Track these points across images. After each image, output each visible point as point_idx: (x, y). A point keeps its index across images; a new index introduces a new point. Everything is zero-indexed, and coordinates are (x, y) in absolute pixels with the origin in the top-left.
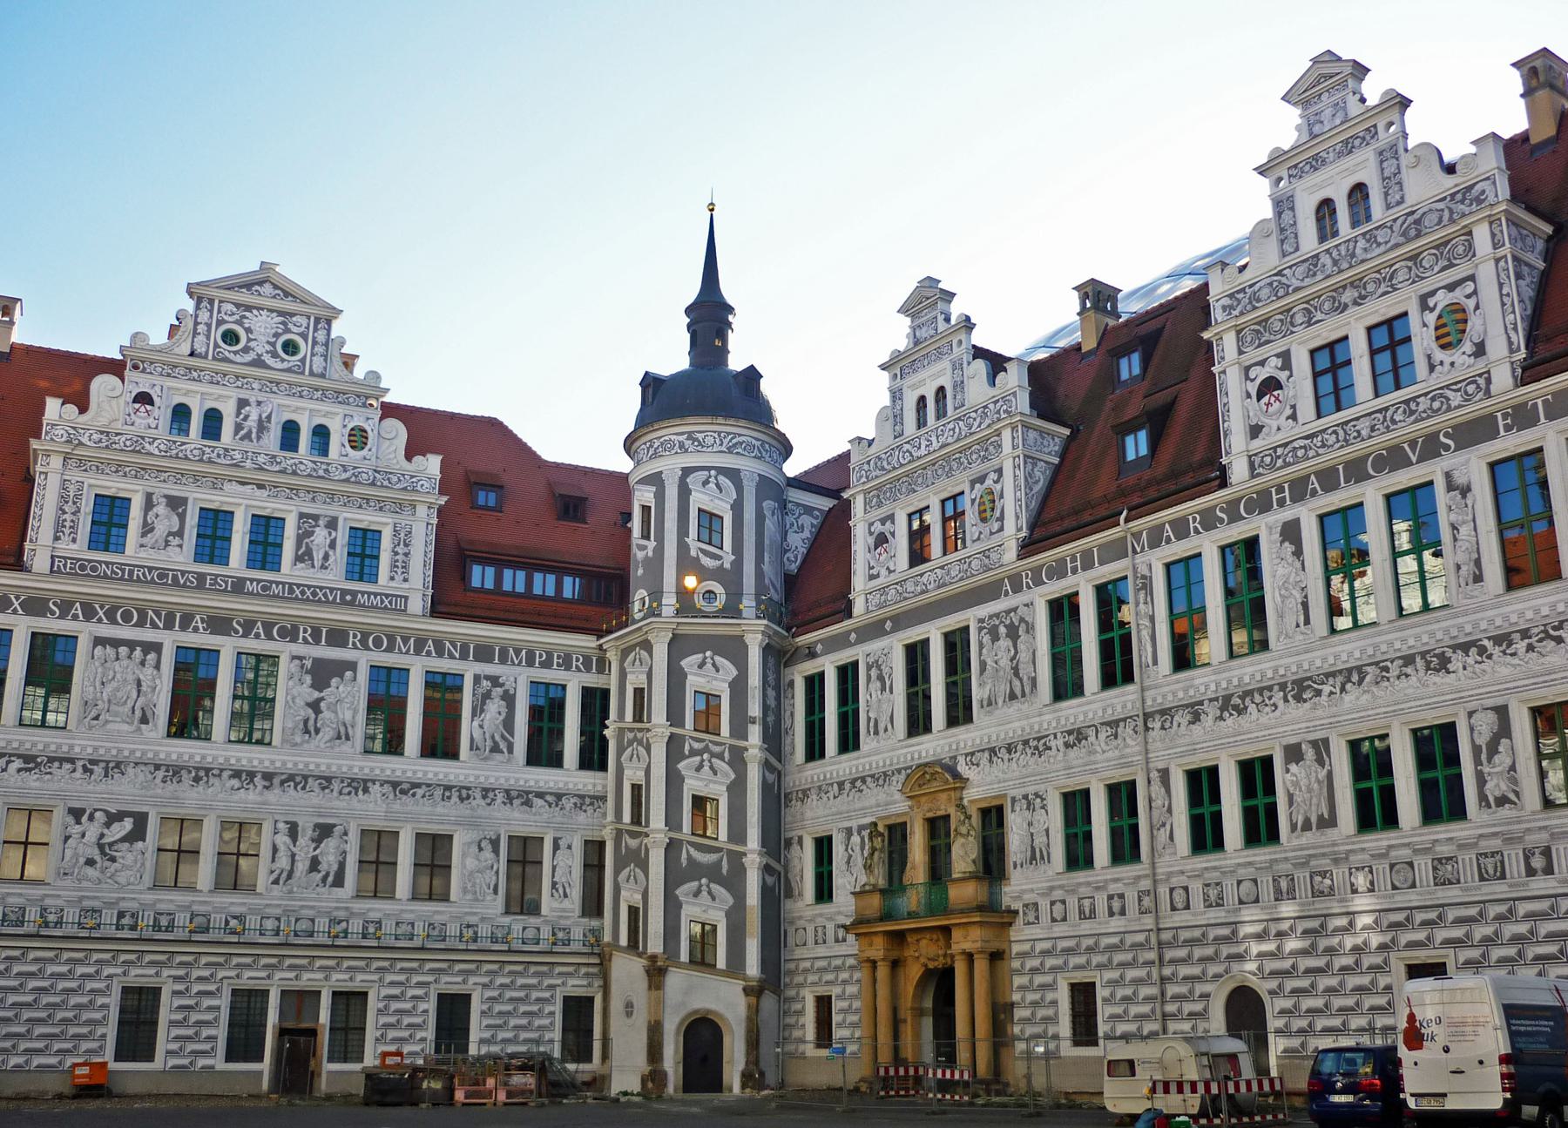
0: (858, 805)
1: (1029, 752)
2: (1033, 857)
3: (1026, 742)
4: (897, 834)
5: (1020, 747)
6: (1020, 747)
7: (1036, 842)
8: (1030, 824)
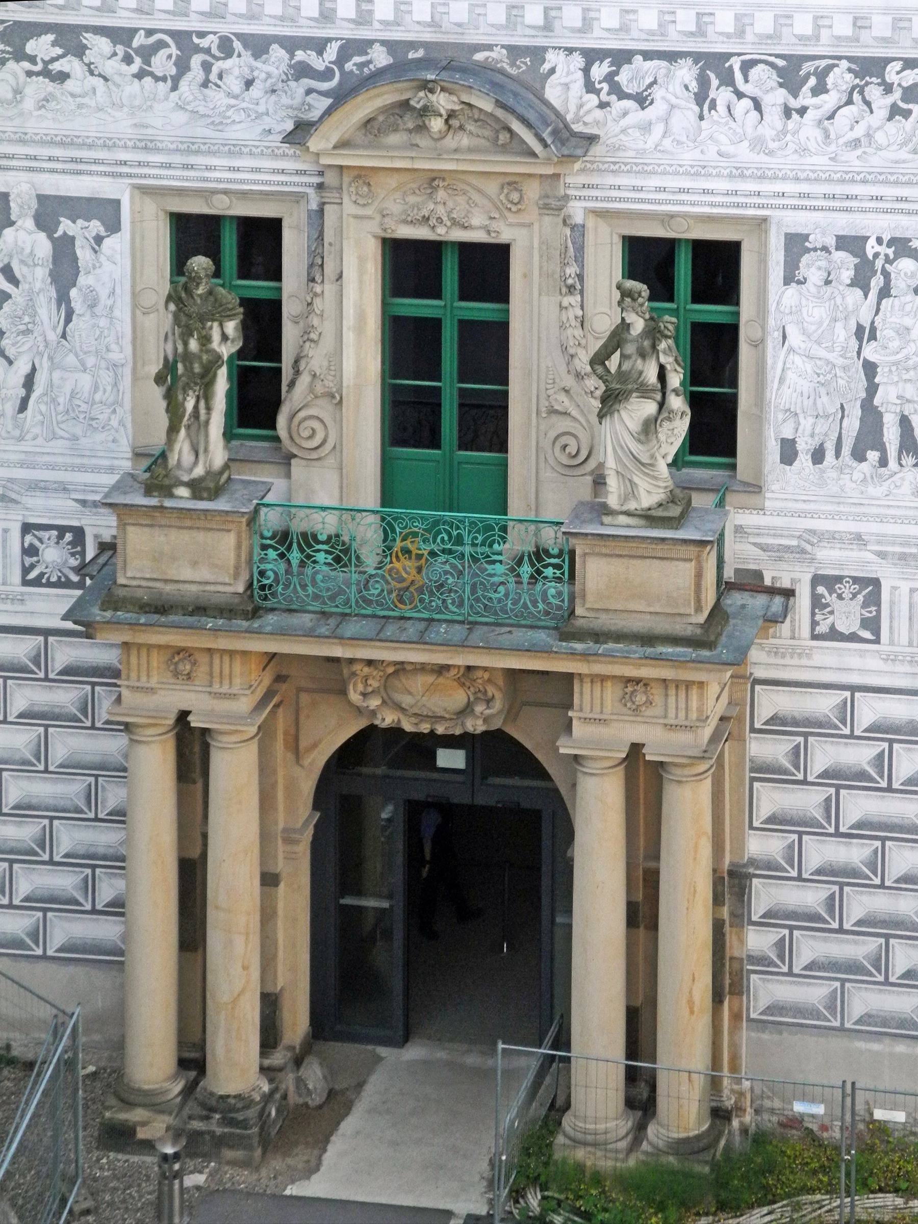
0: (42, 124)
1: (881, 102)
2: (869, 438)
3: (869, 68)
4: (231, 252)
5: (841, 78)
6: (841, 78)
7: (886, 397)
8: (865, 334)
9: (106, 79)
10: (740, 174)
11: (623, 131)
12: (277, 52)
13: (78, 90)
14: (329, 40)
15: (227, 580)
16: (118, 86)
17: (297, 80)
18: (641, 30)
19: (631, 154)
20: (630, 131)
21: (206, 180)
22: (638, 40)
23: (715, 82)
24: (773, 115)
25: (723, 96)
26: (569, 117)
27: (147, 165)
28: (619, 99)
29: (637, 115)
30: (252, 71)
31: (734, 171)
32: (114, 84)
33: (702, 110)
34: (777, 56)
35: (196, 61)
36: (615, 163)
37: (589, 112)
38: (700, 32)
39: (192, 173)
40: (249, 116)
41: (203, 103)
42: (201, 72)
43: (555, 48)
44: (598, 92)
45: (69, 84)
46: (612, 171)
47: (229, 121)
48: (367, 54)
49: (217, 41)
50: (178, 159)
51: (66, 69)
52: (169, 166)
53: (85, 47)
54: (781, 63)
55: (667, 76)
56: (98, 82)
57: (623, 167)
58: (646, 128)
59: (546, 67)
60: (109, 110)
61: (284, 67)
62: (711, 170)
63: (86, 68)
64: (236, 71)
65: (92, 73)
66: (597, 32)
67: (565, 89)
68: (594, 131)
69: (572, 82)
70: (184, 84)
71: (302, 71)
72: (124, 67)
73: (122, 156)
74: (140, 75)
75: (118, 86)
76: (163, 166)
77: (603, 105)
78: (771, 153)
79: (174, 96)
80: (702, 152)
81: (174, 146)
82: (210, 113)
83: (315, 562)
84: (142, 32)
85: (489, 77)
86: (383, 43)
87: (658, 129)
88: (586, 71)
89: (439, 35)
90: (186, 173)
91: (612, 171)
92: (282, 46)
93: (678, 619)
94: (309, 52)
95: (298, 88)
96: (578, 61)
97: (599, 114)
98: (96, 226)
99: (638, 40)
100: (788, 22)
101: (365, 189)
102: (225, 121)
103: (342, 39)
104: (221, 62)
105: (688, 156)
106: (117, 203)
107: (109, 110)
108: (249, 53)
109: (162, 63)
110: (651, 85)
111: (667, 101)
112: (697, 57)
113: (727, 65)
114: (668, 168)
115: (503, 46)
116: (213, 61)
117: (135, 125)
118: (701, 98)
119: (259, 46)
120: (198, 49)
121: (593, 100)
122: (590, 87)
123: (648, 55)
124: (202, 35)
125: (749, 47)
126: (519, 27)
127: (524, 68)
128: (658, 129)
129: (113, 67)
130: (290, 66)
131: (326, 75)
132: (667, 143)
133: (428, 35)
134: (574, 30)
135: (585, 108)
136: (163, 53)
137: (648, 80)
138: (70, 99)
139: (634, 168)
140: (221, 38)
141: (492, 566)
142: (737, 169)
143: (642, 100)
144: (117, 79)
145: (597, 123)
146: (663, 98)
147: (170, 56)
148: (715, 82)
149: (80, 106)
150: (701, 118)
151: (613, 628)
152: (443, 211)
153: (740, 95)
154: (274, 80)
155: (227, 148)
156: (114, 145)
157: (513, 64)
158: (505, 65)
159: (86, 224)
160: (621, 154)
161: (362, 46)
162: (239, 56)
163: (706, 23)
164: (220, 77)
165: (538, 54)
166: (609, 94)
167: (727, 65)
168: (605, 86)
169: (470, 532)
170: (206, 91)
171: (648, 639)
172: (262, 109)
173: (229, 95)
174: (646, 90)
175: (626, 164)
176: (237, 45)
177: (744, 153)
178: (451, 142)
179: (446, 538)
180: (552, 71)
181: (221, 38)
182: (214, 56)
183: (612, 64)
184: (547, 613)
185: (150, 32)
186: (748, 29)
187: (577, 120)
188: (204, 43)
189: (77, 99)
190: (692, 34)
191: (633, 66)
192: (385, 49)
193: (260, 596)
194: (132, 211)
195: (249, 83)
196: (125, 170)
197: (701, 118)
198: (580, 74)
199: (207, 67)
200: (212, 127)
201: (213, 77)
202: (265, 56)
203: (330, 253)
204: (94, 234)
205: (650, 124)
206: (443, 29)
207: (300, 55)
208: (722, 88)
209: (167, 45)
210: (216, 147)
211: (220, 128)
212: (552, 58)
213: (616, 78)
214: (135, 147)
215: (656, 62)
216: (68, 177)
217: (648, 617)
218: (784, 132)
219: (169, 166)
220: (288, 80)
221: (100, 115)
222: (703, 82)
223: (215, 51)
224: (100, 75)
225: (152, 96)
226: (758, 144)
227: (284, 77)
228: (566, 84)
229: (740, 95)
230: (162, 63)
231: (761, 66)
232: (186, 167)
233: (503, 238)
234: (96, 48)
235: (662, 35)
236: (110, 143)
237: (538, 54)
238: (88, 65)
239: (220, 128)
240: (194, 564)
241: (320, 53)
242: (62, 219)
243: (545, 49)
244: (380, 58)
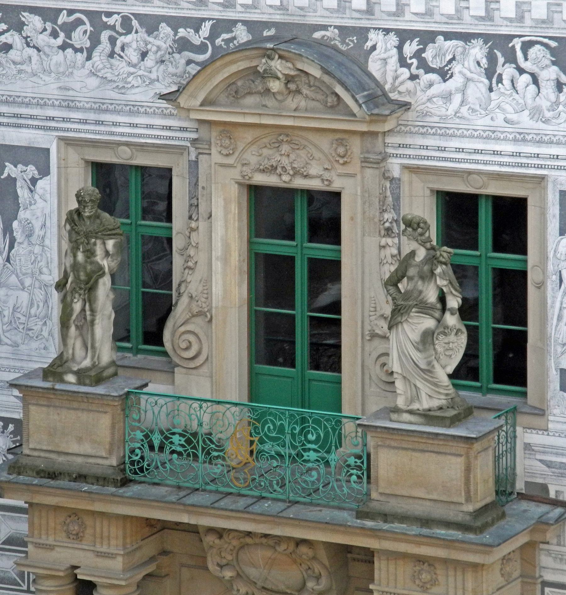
9: (39, 50)
10: (522, 138)
11: (429, 100)
12: (165, 29)
13: (18, 59)
14: (204, 20)
15: (104, 454)
16: (48, 56)
17: (179, 53)
18: (442, 15)
19: (436, 119)
20: (435, 100)
21: (112, 134)
22: (440, 23)
23: (501, 60)
24: (548, 89)
25: (508, 71)
26: (387, 87)
27: (69, 120)
28: (426, 73)
29: (440, 87)
30: (146, 45)
31: (518, 136)
32: (45, 53)
33: (491, 84)
34: (550, 38)
35: (105, 36)
36: (423, 127)
37: (402, 83)
38: (488, 17)
39: (102, 128)
40: (144, 82)
41: (110, 70)
42: (108, 45)
43: (375, 29)
44: (409, 66)
45: (13, 54)
46: (422, 134)
47: (129, 86)
48: (232, 32)
49: (120, 20)
50: (92, 116)
51: (10, 41)
52: (85, 122)
53: (23, 24)
54: (553, 44)
55: (463, 53)
56: (32, 52)
57: (430, 130)
58: (447, 97)
59: (369, 44)
60: (41, 76)
61: (170, 42)
62: (499, 134)
63: (24, 41)
64: (134, 45)
65: (28, 45)
66: (408, 16)
67: (383, 63)
68: (407, 99)
69: (389, 57)
70: (96, 54)
71: (183, 45)
72: (52, 40)
73: (51, 113)
74: (63, 47)
75: (48, 56)
76: (81, 121)
77: (413, 77)
78: (547, 121)
79: (89, 63)
80: (492, 119)
81: (88, 106)
82: (116, 78)
83: (171, 443)
84: (65, 12)
85: (324, 52)
86: (245, 23)
87: (457, 99)
88: (400, 48)
89: (286, 17)
90: (98, 128)
91: (422, 134)
92: (168, 25)
93: (452, 507)
94: (188, 30)
95: (180, 59)
96: (393, 39)
97: (410, 85)
98: (32, 170)
99: (440, 23)
100: (559, 9)
101: (227, 141)
102: (126, 86)
103: (213, 19)
104: (123, 37)
105: (481, 122)
106: (48, 150)
107: (41, 76)
108: (144, 30)
109: (79, 38)
110: (450, 62)
111: (464, 75)
112: (486, 38)
113: (510, 45)
114: (465, 132)
115: (336, 27)
116: (117, 36)
117: (60, 88)
118: (490, 73)
119: (151, 24)
120: (106, 27)
121: (405, 73)
122: (403, 62)
123: (448, 36)
124: (109, 14)
125: (527, 31)
126: (347, 11)
127: (352, 45)
128: (457, 99)
129: (43, 40)
130: (174, 41)
131: (202, 49)
132: (464, 111)
133: (278, 17)
134: (389, 14)
135: (400, 79)
136: (80, 29)
137: (449, 57)
138: (13, 66)
139: (439, 131)
140: (122, 17)
141: (307, 454)
142: (520, 134)
143: (444, 74)
144: (46, 49)
145: (409, 92)
146: (460, 72)
147: (85, 32)
148: (501, 60)
149: (20, 72)
150: (491, 90)
151: (399, 511)
152: (287, 162)
153: (521, 71)
154: (163, 52)
155: (128, 108)
156: (45, 104)
157: (343, 42)
158: (337, 42)
159: (25, 168)
160: (428, 119)
161: (229, 25)
162: (137, 32)
163: (494, 10)
164: (123, 49)
165: (362, 33)
166: (418, 68)
167: (510, 45)
168: (414, 61)
169: (289, 423)
170: (113, 61)
171: (426, 522)
172: (153, 76)
173: (129, 64)
174: (446, 65)
175: (432, 128)
176: (135, 23)
177: (525, 120)
178: (292, 102)
179: (272, 427)
180: (374, 48)
181: (122, 17)
182: (118, 33)
183: (420, 43)
184: (349, 496)
185: (71, 12)
186: (527, 15)
187: (394, 89)
188: (110, 21)
189: (18, 66)
190: (482, 18)
191: (437, 45)
192: (245, 28)
193: (131, 470)
194: (59, 158)
195: (144, 55)
196: (53, 124)
197: (491, 90)
198: (395, 51)
199: (113, 41)
200: (116, 90)
201: (117, 49)
202: (155, 33)
203: (203, 195)
204: (30, 177)
205: (451, 94)
206: (289, 12)
207: (182, 32)
208: (507, 65)
209: (83, 23)
210: (120, 107)
211: (123, 91)
212: (374, 37)
213: (423, 55)
214: (60, 106)
215: (454, 42)
216: (11, 129)
217: (428, 503)
218: (557, 103)
219: (85, 122)
220: (173, 52)
221: (34, 79)
222: (492, 59)
223: (118, 28)
224: (34, 47)
225: (72, 64)
226: (536, 113)
227: (170, 50)
228: (385, 60)
229: (521, 71)
230: (79, 38)
231: (538, 47)
232: (98, 123)
233: (335, 186)
234: (31, 25)
235: (459, 19)
236: (42, 102)
237: (362, 33)
238: (26, 38)
239: (123, 91)
240: (80, 440)
241: (197, 31)
242: (7, 164)
243: (367, 30)
244: (242, 35)
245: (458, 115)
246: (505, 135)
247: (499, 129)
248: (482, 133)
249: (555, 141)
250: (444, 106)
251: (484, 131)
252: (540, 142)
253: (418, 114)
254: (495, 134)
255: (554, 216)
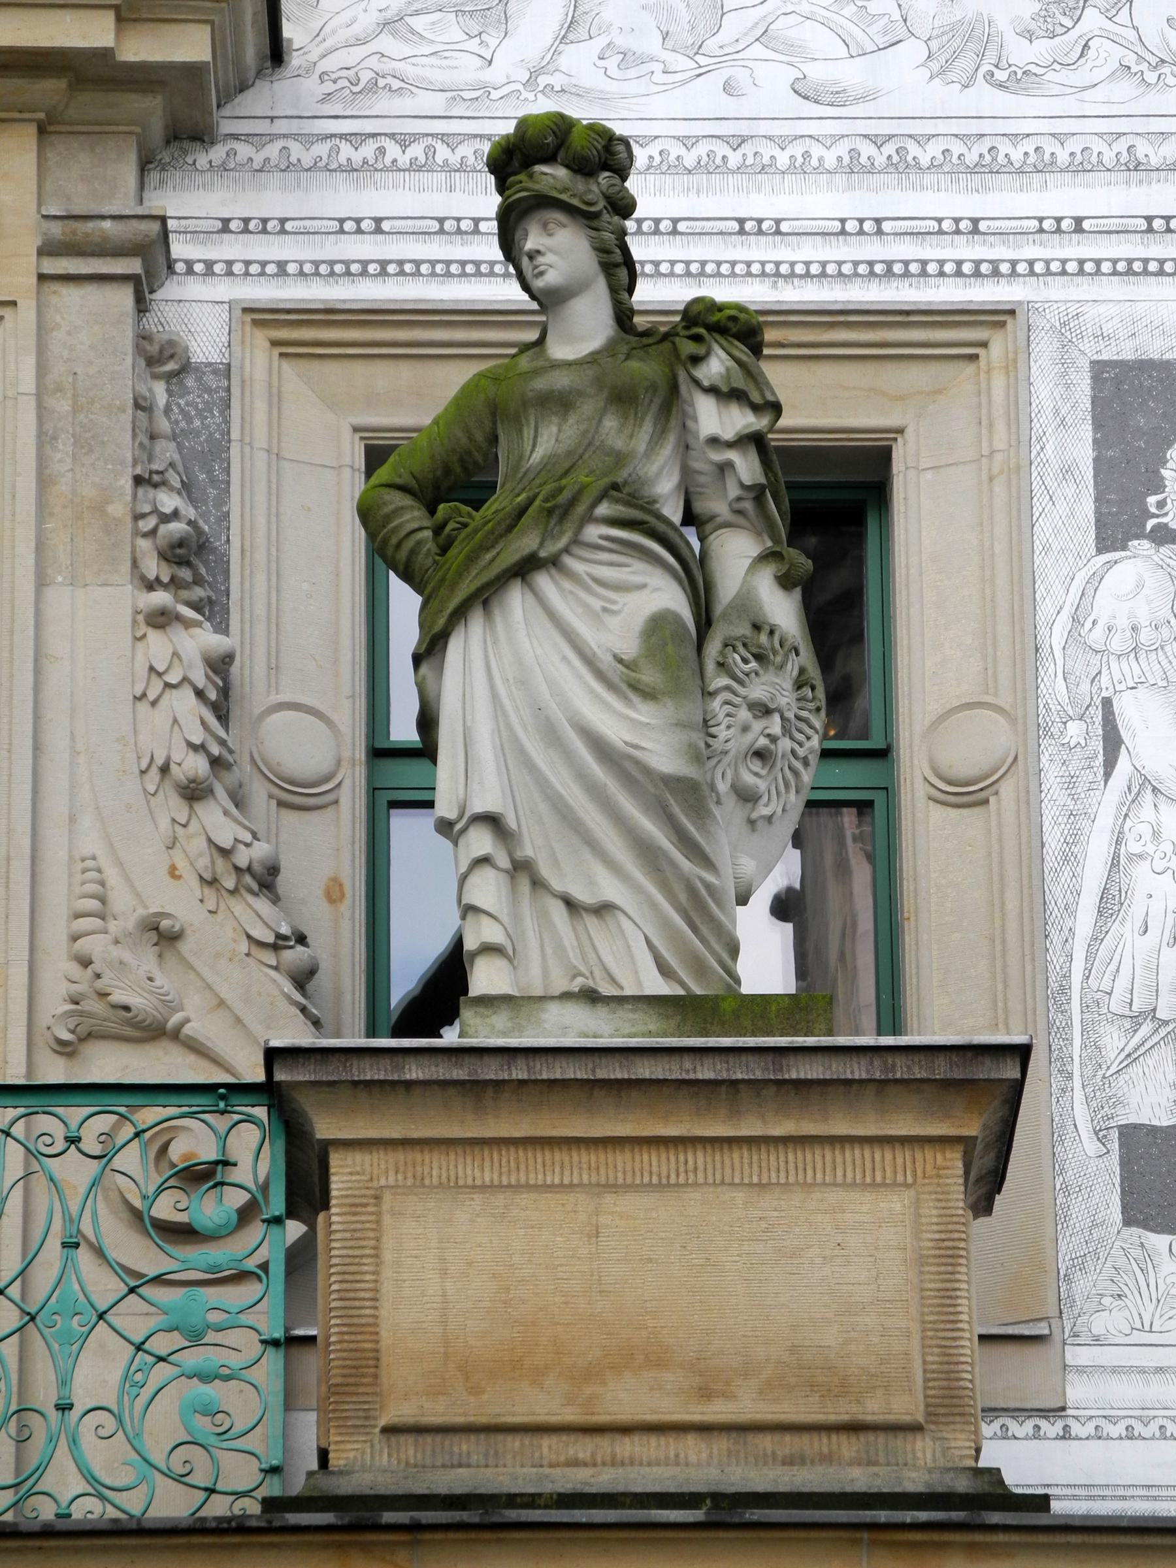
19: (433, 103)
31: (867, 150)
46: (350, 169)
62: (768, 151)
78: (1020, 81)
80: (728, 88)
91: (350, 169)
139: (443, 153)
142: (878, 141)
160: (382, 104)
175: (404, 141)
245: (543, 80)
246: (797, 150)
247: (764, 128)
248: (676, 150)
249: (1063, 158)
250: (473, 45)
251: (687, 142)
252: (988, 169)
253: (329, 87)
254: (748, 149)
255: (1067, 471)
